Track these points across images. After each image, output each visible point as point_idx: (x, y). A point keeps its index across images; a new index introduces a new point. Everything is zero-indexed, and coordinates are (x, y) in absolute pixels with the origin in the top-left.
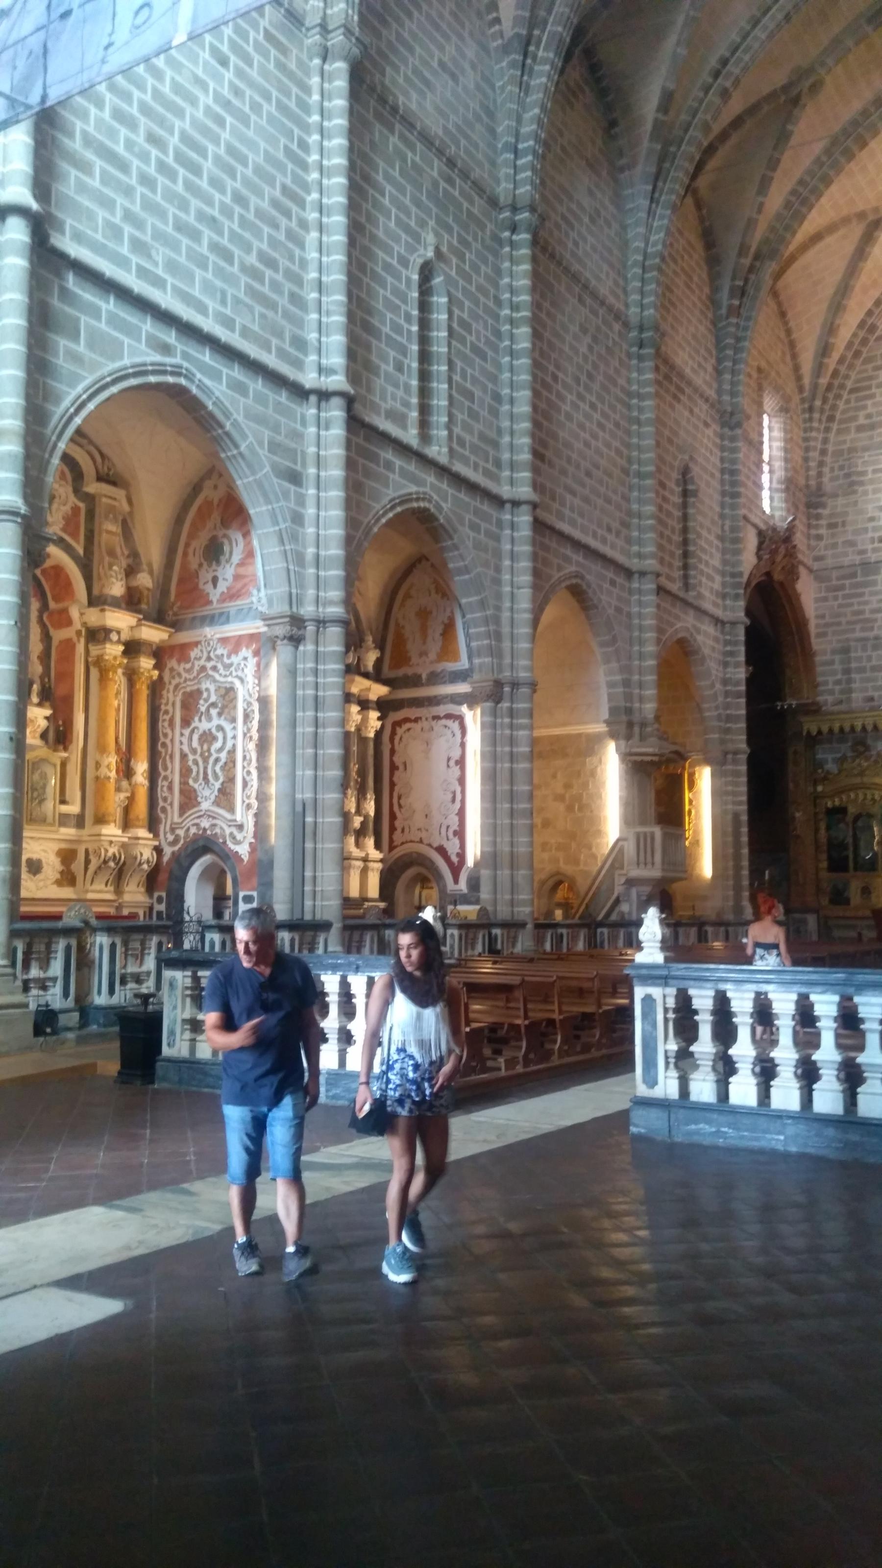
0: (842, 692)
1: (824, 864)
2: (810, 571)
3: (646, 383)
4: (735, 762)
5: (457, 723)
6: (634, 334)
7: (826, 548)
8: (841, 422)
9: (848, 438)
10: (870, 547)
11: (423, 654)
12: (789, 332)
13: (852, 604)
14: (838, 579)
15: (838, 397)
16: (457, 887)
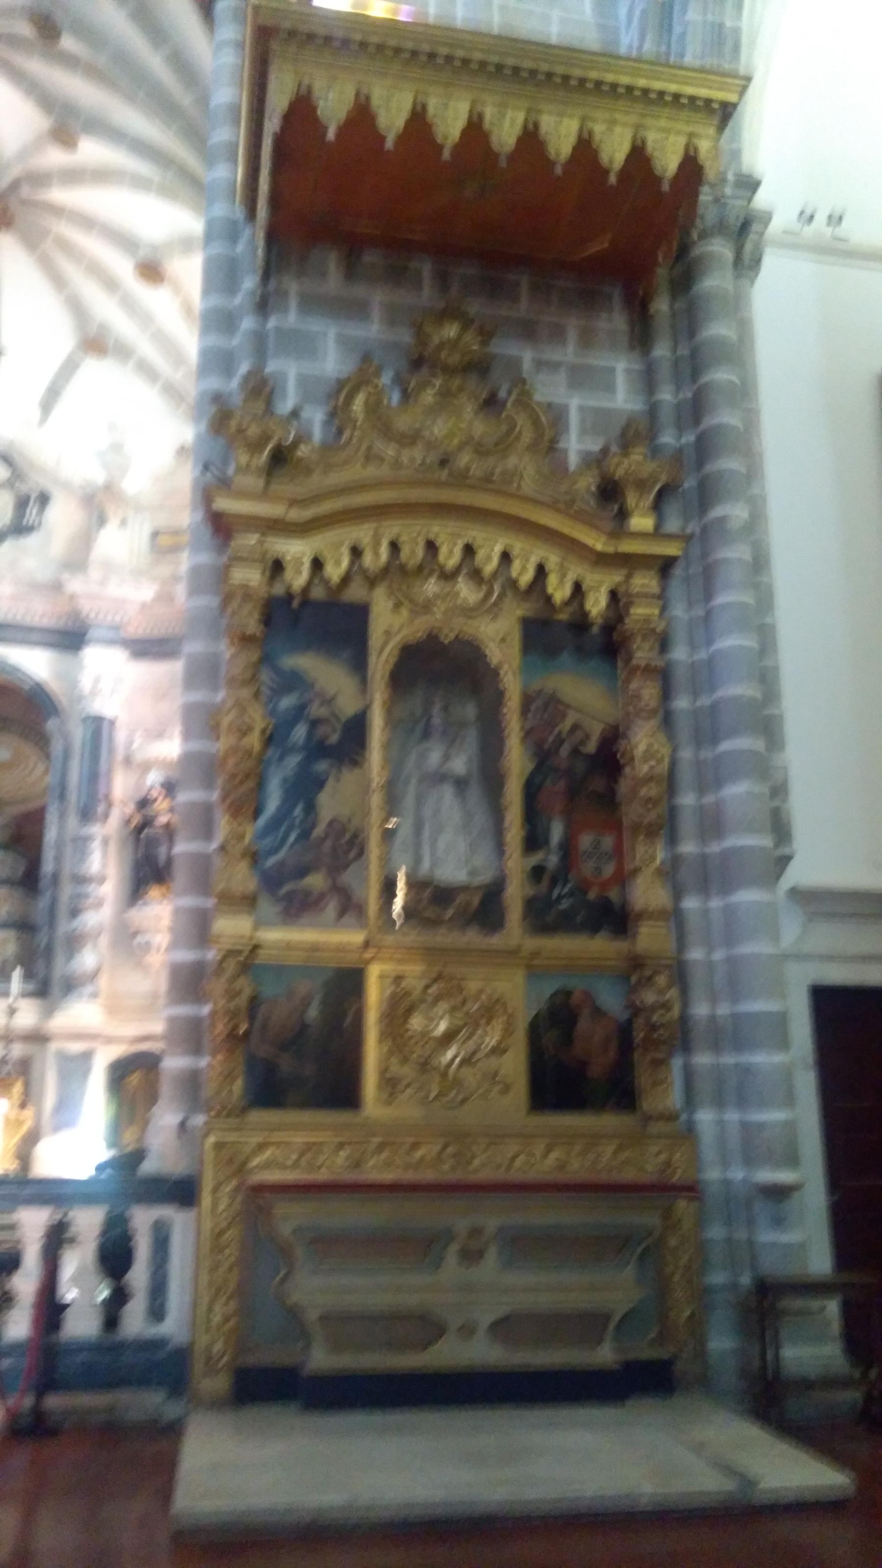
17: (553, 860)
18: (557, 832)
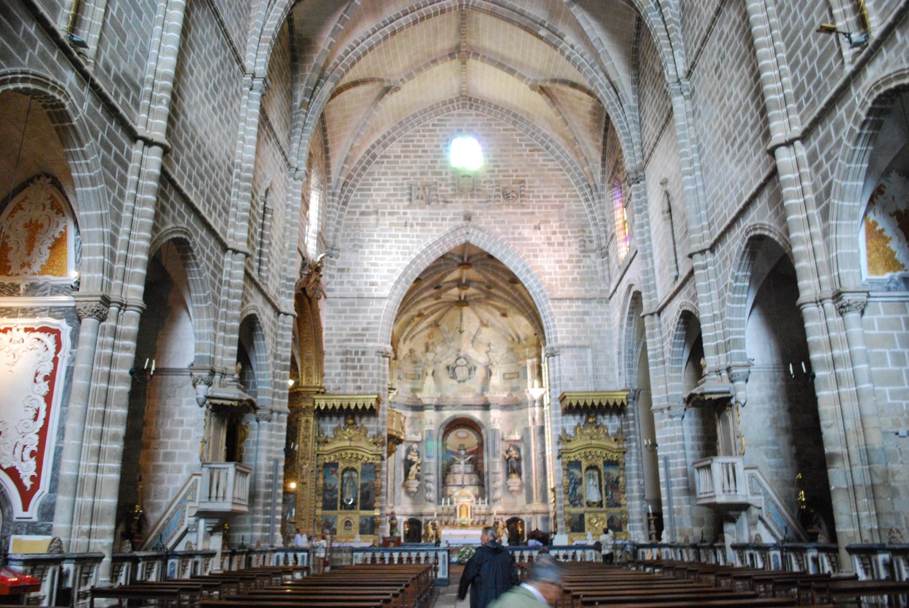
0: (341, 381)
1: (320, 504)
2: (326, 297)
3: (252, 115)
4: (278, 420)
5: (53, 336)
6: (248, 78)
7: (336, 284)
8: (351, 207)
10: (364, 287)
11: (26, 265)
12: (326, 142)
13: (350, 323)
14: (342, 305)
15: (350, 191)
16: (26, 514)
18: (610, 493)
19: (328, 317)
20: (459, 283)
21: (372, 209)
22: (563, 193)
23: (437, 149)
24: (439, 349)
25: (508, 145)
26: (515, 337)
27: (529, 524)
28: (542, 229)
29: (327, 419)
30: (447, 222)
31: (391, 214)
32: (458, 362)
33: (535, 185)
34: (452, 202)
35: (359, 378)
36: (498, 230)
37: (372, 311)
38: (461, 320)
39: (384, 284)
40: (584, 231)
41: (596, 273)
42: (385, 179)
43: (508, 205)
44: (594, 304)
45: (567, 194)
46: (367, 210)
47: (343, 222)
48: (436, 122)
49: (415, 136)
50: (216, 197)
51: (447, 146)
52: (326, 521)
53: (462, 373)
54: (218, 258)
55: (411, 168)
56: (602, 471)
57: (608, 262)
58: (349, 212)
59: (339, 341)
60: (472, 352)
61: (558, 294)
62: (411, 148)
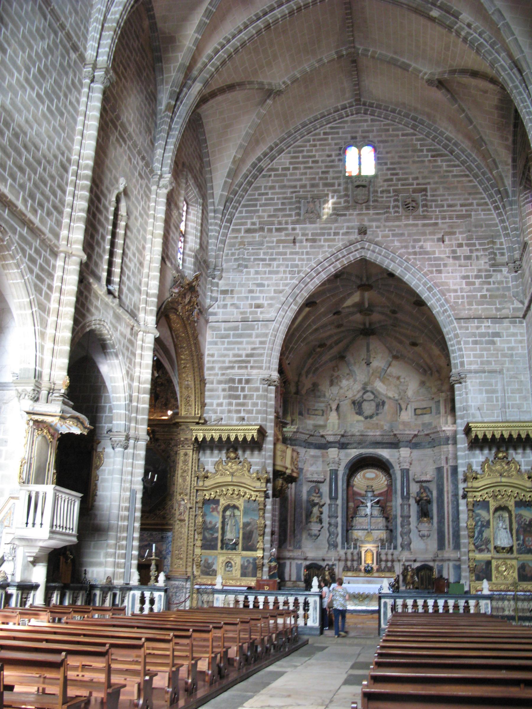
1: (199, 543)
7: (218, 307)
8: (236, 225)
9: (240, 235)
13: (233, 349)
14: (225, 330)
15: (236, 208)
17: (521, 542)
18: (522, 537)
19: (211, 343)
20: (360, 307)
21: (257, 226)
22: (470, 201)
23: (328, 159)
24: (344, 383)
25: (407, 151)
26: (426, 368)
27: (440, 571)
28: (447, 242)
29: (208, 452)
30: (340, 237)
31: (278, 230)
32: (365, 397)
33: (438, 193)
34: (345, 215)
35: (242, 408)
36: (397, 244)
37: (257, 336)
38: (368, 350)
39: (270, 305)
40: (494, 243)
41: (508, 289)
42: (272, 194)
43: (407, 217)
44: (506, 323)
45: (475, 202)
46: (253, 227)
47: (227, 241)
48: (328, 131)
49: (306, 146)
50: (43, 194)
51: (340, 155)
52: (206, 561)
53: (368, 408)
54: (47, 262)
55: (301, 180)
56: (513, 513)
57: (522, 276)
58: (233, 230)
59: (221, 368)
60: (380, 386)
61: (465, 313)
62: (301, 159)
